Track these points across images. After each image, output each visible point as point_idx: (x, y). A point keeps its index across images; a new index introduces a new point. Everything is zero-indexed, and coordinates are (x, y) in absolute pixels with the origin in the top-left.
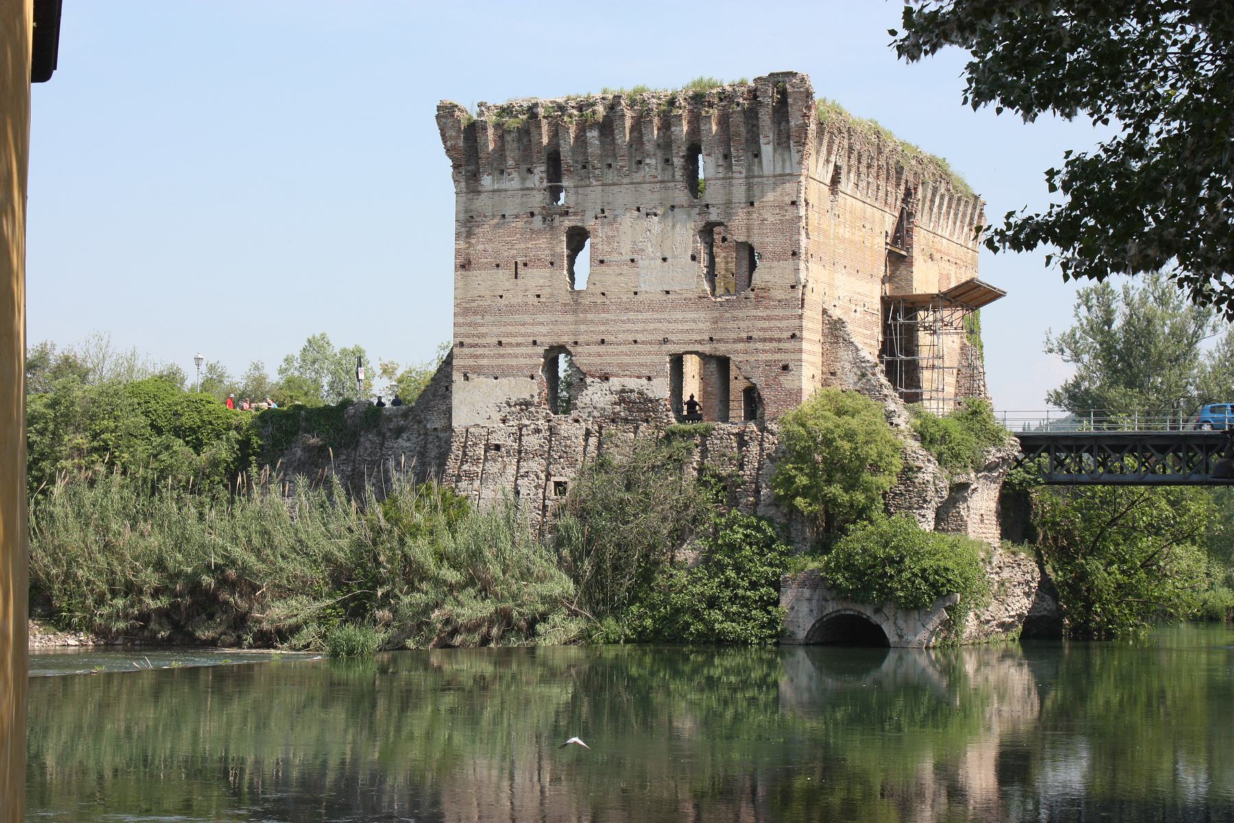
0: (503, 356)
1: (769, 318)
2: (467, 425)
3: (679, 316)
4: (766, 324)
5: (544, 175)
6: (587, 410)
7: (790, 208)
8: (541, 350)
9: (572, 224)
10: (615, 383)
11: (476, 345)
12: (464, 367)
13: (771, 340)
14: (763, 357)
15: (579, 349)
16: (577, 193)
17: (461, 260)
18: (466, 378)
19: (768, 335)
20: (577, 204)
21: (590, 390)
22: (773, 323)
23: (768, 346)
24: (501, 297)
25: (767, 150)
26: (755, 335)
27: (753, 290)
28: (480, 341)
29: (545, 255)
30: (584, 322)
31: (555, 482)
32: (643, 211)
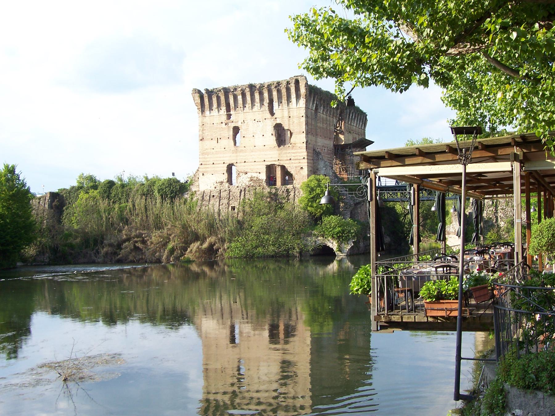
2: (205, 189)
5: (225, 110)
6: (241, 184)
7: (302, 118)
8: (226, 165)
10: (249, 175)
11: (206, 164)
12: (202, 171)
13: (297, 159)
14: (295, 165)
15: (237, 164)
17: (201, 138)
19: (296, 158)
21: (242, 177)
22: (297, 154)
31: (232, 207)
32: (256, 120)
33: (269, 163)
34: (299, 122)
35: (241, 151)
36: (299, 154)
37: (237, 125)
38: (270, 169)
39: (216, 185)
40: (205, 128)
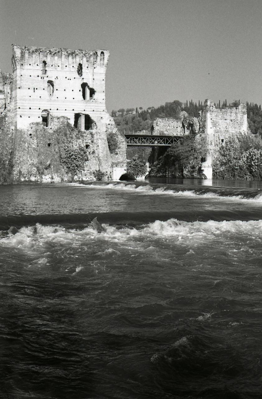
1: (98, 106)
4: (97, 108)
5: (42, 66)
9: (49, 80)
11: (24, 109)
13: (99, 111)
14: (97, 115)
18: (21, 116)
19: (98, 110)
23: (98, 113)
24: (30, 96)
26: (95, 110)
27: (94, 99)
28: (25, 108)
32: (67, 78)
33: (77, 112)
35: (55, 101)
37: (51, 80)
38: (77, 116)
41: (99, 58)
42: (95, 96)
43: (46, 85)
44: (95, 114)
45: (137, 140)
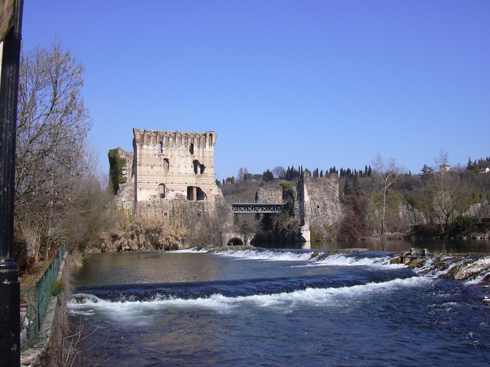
0: (149, 185)
1: (208, 180)
3: (189, 178)
4: (207, 181)
8: (158, 184)
10: (175, 192)
13: (208, 184)
15: (167, 184)
16: (166, 151)
18: (140, 189)
19: (207, 183)
20: (166, 153)
21: (170, 193)
22: (209, 181)
25: (207, 146)
28: (144, 182)
29: (159, 164)
30: (168, 179)
31: (164, 213)
32: (181, 156)
33: (190, 185)
34: (210, 161)
35: (170, 176)
36: (209, 181)
37: (166, 158)
38: (190, 189)
39: (150, 197)
40: (142, 157)
41: (208, 139)
42: (206, 171)
43: (163, 162)
44: (205, 186)
45: (242, 208)
